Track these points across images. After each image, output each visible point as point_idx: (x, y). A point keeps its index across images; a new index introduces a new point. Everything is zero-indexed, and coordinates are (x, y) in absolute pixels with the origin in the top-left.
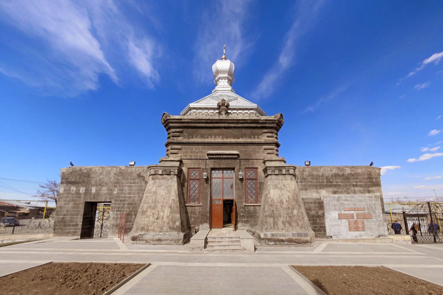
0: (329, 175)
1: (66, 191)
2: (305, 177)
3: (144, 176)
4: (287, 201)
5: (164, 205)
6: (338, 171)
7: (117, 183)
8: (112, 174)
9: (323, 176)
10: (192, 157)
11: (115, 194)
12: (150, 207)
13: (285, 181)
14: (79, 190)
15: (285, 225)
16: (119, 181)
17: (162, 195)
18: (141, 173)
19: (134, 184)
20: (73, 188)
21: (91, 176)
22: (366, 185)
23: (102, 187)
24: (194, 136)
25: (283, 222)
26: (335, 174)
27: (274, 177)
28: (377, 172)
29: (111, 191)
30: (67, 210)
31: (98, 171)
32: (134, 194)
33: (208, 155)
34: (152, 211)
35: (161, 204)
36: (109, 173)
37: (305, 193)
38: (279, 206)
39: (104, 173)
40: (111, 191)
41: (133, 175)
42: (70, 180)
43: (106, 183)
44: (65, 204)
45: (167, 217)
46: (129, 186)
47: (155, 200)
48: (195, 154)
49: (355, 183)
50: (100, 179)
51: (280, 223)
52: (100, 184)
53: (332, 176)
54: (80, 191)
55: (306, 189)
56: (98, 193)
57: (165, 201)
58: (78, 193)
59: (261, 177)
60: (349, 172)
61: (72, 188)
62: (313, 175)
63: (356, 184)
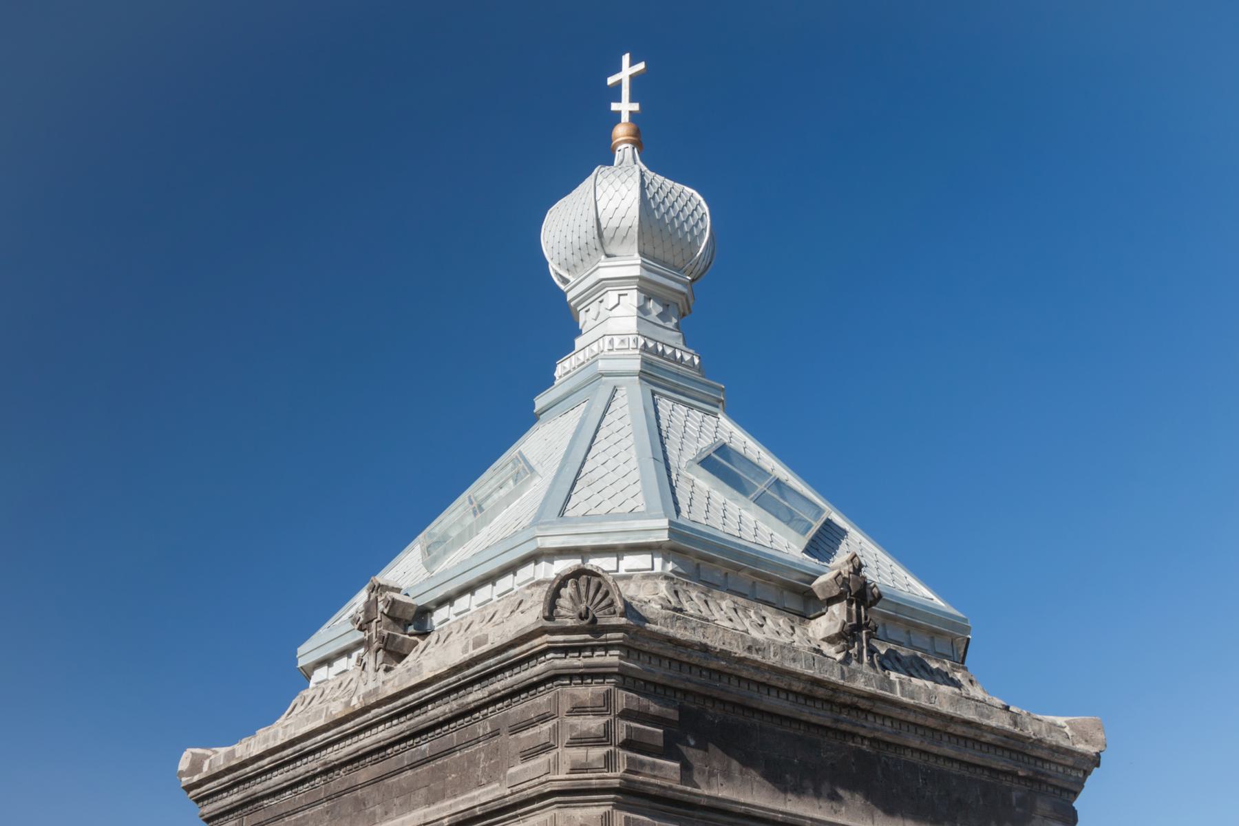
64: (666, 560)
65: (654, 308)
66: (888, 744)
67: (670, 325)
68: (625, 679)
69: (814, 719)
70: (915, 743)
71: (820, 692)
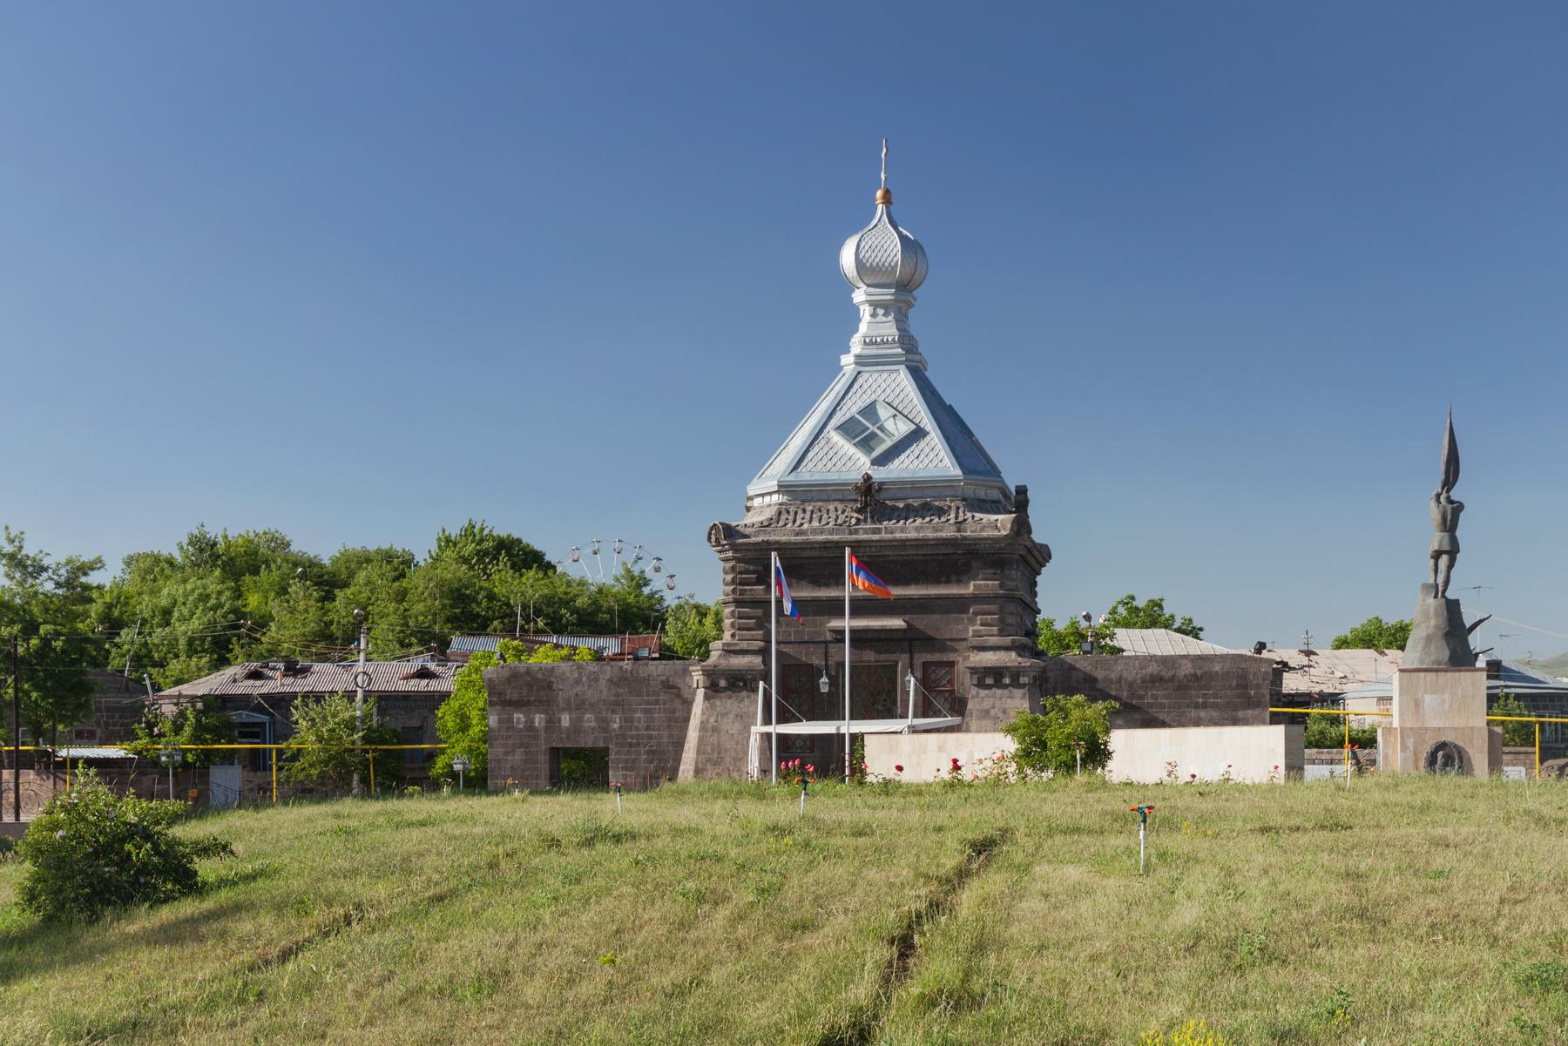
0: (1135, 681)
1: (503, 723)
3: (679, 685)
5: (739, 756)
6: (1162, 667)
7: (617, 703)
8: (603, 683)
9: (1120, 682)
10: (790, 635)
11: (614, 730)
12: (709, 760)
13: (1008, 700)
14: (533, 722)
16: (620, 698)
17: (733, 735)
18: (671, 679)
19: (657, 705)
20: (519, 717)
21: (555, 686)
22: (1229, 703)
23: (584, 714)
26: (1152, 675)
28: (1263, 670)
29: (604, 724)
30: (512, 767)
31: (569, 676)
32: (659, 729)
34: (715, 769)
35: (733, 755)
36: (596, 680)
39: (584, 679)
40: (604, 724)
41: (652, 683)
42: (508, 698)
43: (590, 704)
44: (506, 753)
46: (646, 711)
47: (718, 745)
48: (798, 627)
49: (1200, 700)
50: (577, 694)
52: (579, 706)
53: (1143, 682)
54: (534, 723)
56: (576, 729)
57: (739, 747)
58: (530, 727)
59: (962, 684)
60: (1188, 672)
61: (515, 715)
63: (1203, 702)
64: (783, 495)
65: (881, 312)
66: (878, 556)
67: (890, 318)
68: (738, 560)
69: (831, 555)
70: (891, 553)
71: (829, 545)
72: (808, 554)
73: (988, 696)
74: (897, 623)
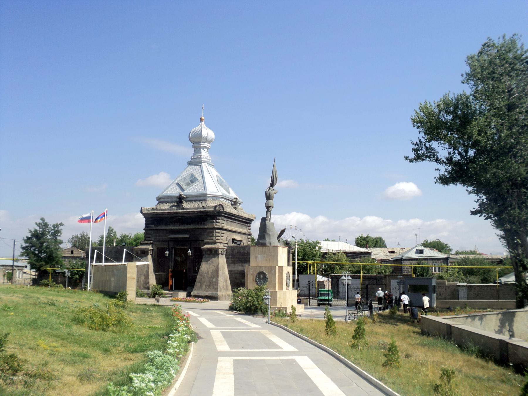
2: (234, 254)
4: (211, 273)
15: (206, 288)
24: (161, 224)
25: (206, 286)
27: (207, 256)
33: (170, 238)
37: (234, 266)
38: (206, 276)
39: (109, 251)
45: (143, 281)
51: (204, 287)
55: (235, 264)
62: (240, 252)
72: (164, 216)
73: (208, 257)
74: (187, 236)
